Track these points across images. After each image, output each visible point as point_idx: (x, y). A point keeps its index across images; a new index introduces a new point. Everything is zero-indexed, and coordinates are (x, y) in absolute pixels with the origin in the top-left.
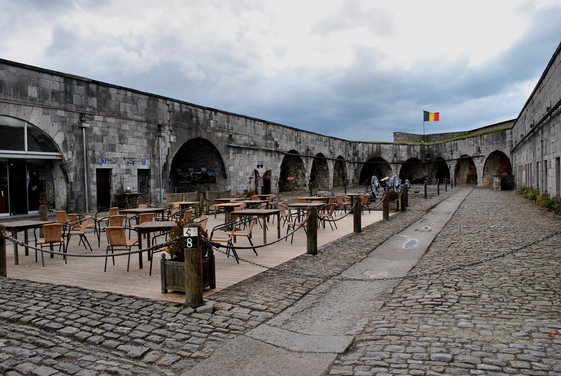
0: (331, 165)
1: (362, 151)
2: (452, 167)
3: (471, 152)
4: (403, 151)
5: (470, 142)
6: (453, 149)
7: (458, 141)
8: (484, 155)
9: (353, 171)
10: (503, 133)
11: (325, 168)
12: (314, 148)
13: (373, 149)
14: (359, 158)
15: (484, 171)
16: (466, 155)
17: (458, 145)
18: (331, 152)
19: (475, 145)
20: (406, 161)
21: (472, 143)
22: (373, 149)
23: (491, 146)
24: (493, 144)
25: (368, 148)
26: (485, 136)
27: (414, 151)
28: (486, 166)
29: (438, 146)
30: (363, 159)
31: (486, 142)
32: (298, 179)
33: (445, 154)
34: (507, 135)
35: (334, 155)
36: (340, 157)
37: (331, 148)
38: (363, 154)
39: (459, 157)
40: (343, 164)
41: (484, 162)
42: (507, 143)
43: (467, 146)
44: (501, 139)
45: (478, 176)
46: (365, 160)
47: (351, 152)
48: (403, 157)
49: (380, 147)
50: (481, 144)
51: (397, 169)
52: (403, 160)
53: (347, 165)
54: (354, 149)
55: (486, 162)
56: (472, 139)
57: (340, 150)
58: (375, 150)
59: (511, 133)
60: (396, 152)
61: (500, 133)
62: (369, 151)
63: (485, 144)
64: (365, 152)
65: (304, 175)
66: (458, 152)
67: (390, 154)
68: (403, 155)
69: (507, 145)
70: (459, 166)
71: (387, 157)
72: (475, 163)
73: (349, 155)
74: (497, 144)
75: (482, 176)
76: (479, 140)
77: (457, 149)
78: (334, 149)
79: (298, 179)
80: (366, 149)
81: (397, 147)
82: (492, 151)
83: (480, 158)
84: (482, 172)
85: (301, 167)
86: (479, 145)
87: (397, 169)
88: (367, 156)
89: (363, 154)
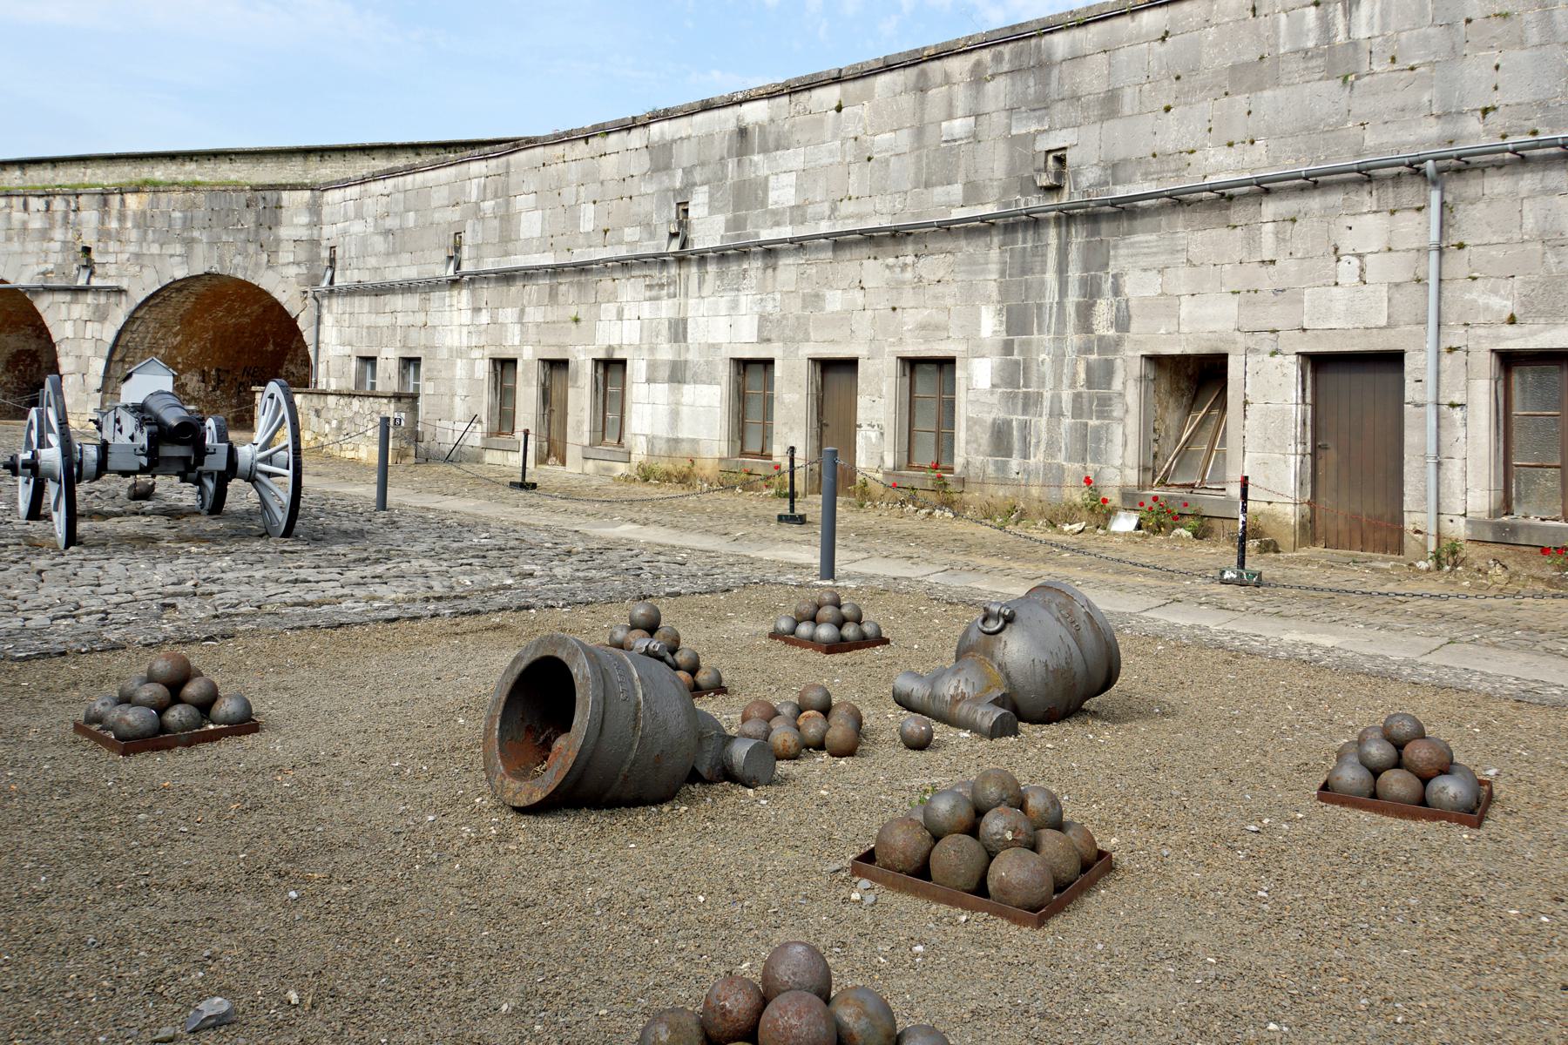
10: (266, 201)
15: (109, 360)
19: (58, 234)
21: (36, 223)
23: (178, 249)
24: (189, 243)
26: (131, 200)
28: (126, 337)
31: (137, 226)
34: (285, 215)
41: (119, 316)
44: (249, 219)
50: (104, 235)
55: (132, 319)
56: (36, 204)
59: (315, 209)
61: (243, 197)
63: (134, 235)
69: (285, 256)
72: (49, 319)
74: (211, 244)
75: (96, 381)
82: (180, 273)
83: (90, 298)
84: (99, 365)
86: (89, 239)
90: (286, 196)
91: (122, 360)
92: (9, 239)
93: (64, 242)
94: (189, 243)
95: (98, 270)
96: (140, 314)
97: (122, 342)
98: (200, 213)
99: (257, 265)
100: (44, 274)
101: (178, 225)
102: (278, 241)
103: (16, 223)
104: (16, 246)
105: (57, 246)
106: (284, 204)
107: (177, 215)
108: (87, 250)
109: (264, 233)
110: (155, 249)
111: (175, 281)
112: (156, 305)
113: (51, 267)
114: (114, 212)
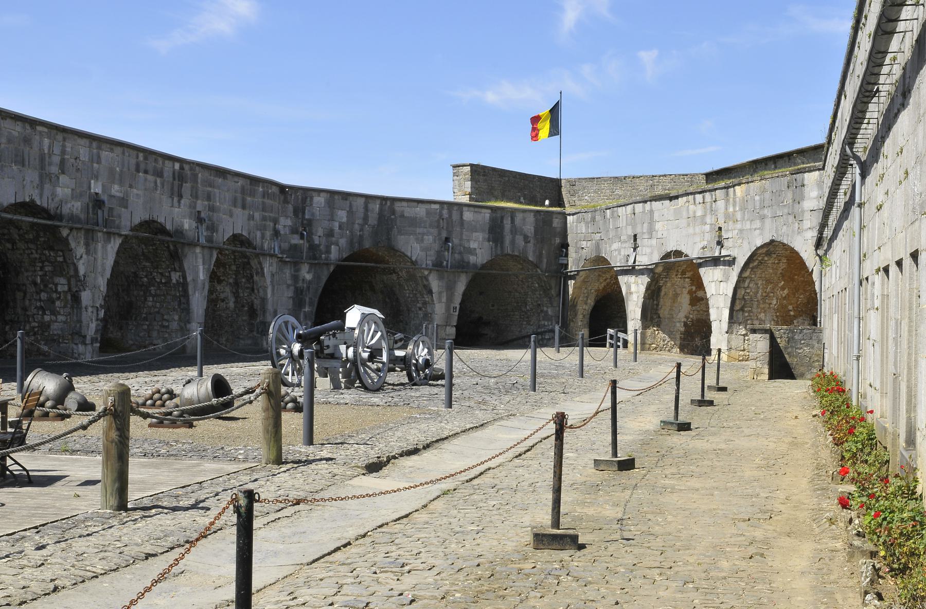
0: (198, 268)
1: (326, 224)
2: (634, 290)
3: (694, 247)
5: (692, 207)
6: (638, 231)
7: (656, 205)
8: (734, 253)
9: (290, 293)
11: (175, 277)
12: (124, 202)
13: (366, 218)
14: (313, 248)
16: (678, 253)
17: (656, 216)
18: (200, 220)
20: (484, 266)
22: (366, 218)
23: (757, 224)
24: (763, 218)
25: (351, 213)
28: (741, 292)
29: (593, 219)
30: (328, 251)
31: (743, 209)
32: (54, 313)
35: (212, 228)
36: (236, 239)
37: (200, 205)
38: (330, 234)
39: (656, 259)
40: (254, 263)
42: (807, 215)
43: (683, 222)
45: (714, 326)
46: (334, 254)
47: (285, 223)
48: (472, 252)
49: (393, 212)
51: (450, 289)
52: (472, 259)
53: (269, 267)
54: (296, 212)
55: (741, 280)
57: (238, 211)
58: (373, 220)
60: (450, 232)
63: (739, 216)
64: (337, 224)
65: (76, 299)
66: (654, 242)
67: (428, 239)
68: (473, 245)
69: (807, 224)
70: (659, 289)
71: (417, 246)
73: (276, 233)
76: (721, 204)
77: (651, 231)
78: (212, 209)
79: (54, 313)
80: (342, 215)
81: (455, 216)
84: (726, 313)
85: (66, 267)
87: (450, 289)
88: (343, 242)
89: (330, 234)
90: (806, 175)
91: (742, 309)
92: (689, 225)
93: (711, 224)
94: (763, 218)
95: (726, 243)
96: (747, 274)
97: (739, 295)
98: (767, 195)
99: (793, 231)
100: (703, 248)
101: (758, 204)
102: (803, 212)
103: (691, 214)
104: (691, 230)
105: (707, 227)
106: (805, 183)
107: (757, 198)
108: (720, 229)
109: (796, 206)
110: (748, 225)
111: (758, 249)
112: (757, 267)
113: (706, 243)
114: (731, 200)
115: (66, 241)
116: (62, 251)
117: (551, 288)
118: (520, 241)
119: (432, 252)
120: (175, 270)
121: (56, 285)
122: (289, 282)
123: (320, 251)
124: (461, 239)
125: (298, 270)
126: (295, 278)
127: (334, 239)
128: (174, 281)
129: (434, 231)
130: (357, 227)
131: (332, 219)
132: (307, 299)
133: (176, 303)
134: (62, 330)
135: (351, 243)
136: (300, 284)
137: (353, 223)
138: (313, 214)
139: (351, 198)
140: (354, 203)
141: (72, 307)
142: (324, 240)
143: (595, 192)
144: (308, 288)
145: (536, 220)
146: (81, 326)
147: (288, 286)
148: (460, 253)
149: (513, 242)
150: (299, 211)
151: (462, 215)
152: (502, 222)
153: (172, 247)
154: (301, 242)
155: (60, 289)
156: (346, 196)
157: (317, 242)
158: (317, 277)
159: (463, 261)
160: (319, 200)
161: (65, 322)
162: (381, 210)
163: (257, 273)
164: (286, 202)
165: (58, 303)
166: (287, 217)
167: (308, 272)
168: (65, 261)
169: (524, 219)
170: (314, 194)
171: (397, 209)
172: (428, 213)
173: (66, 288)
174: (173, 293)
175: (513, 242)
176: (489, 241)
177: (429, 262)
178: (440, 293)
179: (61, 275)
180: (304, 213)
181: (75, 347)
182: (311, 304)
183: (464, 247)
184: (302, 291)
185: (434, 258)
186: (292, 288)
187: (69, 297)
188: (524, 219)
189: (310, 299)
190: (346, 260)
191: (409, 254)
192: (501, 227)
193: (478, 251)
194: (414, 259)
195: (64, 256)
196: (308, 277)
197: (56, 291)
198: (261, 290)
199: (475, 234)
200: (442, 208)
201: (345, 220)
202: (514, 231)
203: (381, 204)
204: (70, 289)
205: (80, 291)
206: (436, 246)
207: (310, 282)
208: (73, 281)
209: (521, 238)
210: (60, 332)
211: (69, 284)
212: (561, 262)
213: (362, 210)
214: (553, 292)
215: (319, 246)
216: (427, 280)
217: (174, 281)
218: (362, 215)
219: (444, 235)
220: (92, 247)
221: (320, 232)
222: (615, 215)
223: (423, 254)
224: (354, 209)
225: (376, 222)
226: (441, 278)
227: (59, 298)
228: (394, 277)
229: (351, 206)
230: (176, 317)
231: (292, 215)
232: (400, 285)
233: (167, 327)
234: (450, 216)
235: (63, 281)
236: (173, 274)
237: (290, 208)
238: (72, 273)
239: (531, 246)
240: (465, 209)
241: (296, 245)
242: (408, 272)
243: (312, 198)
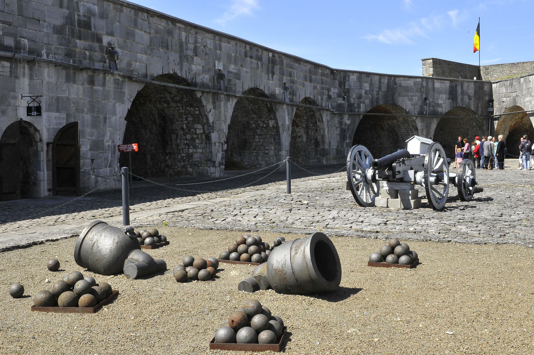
0: (285, 117)
1: (357, 91)
4: (441, 93)
9: (338, 132)
11: (271, 123)
12: (238, 76)
13: (380, 87)
14: (350, 105)
18: (285, 88)
20: (448, 113)
22: (380, 87)
25: (371, 84)
27: (463, 93)
29: (511, 84)
30: (359, 107)
32: (195, 147)
33: (527, 99)
35: (293, 93)
36: (307, 100)
37: (285, 79)
38: (360, 97)
40: (317, 115)
46: (363, 109)
47: (334, 91)
48: (440, 105)
49: (395, 83)
52: (440, 110)
53: (326, 117)
57: (307, 84)
58: (384, 88)
62: (371, 90)
64: (364, 91)
65: (208, 138)
67: (416, 99)
68: (440, 102)
71: (409, 103)
73: (329, 97)
78: (292, 82)
79: (195, 147)
80: (366, 86)
81: (430, 85)
85: (201, 118)
88: (367, 101)
89: (360, 97)
115: (199, 101)
116: (198, 107)
117: (483, 126)
118: (466, 99)
119: (418, 106)
120: (271, 119)
121: (196, 129)
122: (337, 125)
123: (354, 107)
124: (434, 99)
125: (342, 119)
126: (341, 123)
127: (362, 100)
128: (271, 126)
129: (419, 94)
130: (375, 92)
131: (361, 88)
132: (348, 135)
133: (273, 139)
134: (200, 158)
135: (372, 102)
136: (343, 126)
137: (373, 91)
138: (350, 86)
139: (371, 76)
140: (373, 79)
141: (206, 143)
142: (356, 101)
143: (500, 72)
144: (348, 129)
145: (475, 87)
146: (212, 155)
147: (337, 128)
148: (433, 106)
149: (462, 99)
150: (342, 84)
151: (434, 84)
152: (456, 88)
153: (269, 105)
154: (344, 102)
155: (198, 132)
156: (368, 74)
157: (352, 102)
158: (353, 122)
159: (435, 111)
160: (353, 77)
161: (202, 153)
162: (388, 82)
163: (319, 121)
164: (334, 79)
165: (197, 141)
166: (335, 88)
167: (348, 120)
168: (200, 113)
169: (468, 86)
170: (350, 74)
171: (397, 82)
172: (415, 84)
173: (202, 131)
174: (270, 133)
175: (462, 99)
176: (449, 99)
177: (416, 112)
178: (422, 130)
179: (198, 123)
180: (345, 85)
181: (208, 168)
182: (349, 139)
183: (435, 103)
184: (345, 131)
185: (419, 110)
186: (339, 129)
187: (204, 137)
188: (468, 86)
189: (350, 135)
190: (370, 111)
191: (405, 108)
192: (456, 91)
193: (443, 105)
194: (407, 110)
195: (199, 110)
196: (348, 122)
197: (196, 133)
198: (321, 131)
199: (441, 96)
200: (423, 81)
201: (368, 89)
202: (463, 93)
203: (388, 79)
204: (204, 132)
205: (211, 133)
206: (420, 103)
207: (349, 125)
208: (206, 127)
209: (467, 97)
210: (199, 160)
211: (203, 128)
212: (489, 110)
213: (377, 83)
214: (485, 128)
215: (354, 104)
216: (415, 123)
217: (271, 126)
218: (378, 86)
219: (424, 96)
220: (217, 104)
221: (354, 96)
222: (527, 80)
223: (412, 108)
224: (373, 82)
225: (386, 90)
226: (423, 121)
227: (198, 138)
228: (395, 121)
229: (371, 81)
230: (273, 148)
231: (338, 86)
232: (398, 126)
233: (268, 154)
234: (427, 85)
235: (199, 126)
236: (270, 121)
237: (337, 82)
238: (205, 121)
239: (472, 101)
240: (435, 81)
241: (340, 104)
242: (403, 118)
243: (349, 76)
